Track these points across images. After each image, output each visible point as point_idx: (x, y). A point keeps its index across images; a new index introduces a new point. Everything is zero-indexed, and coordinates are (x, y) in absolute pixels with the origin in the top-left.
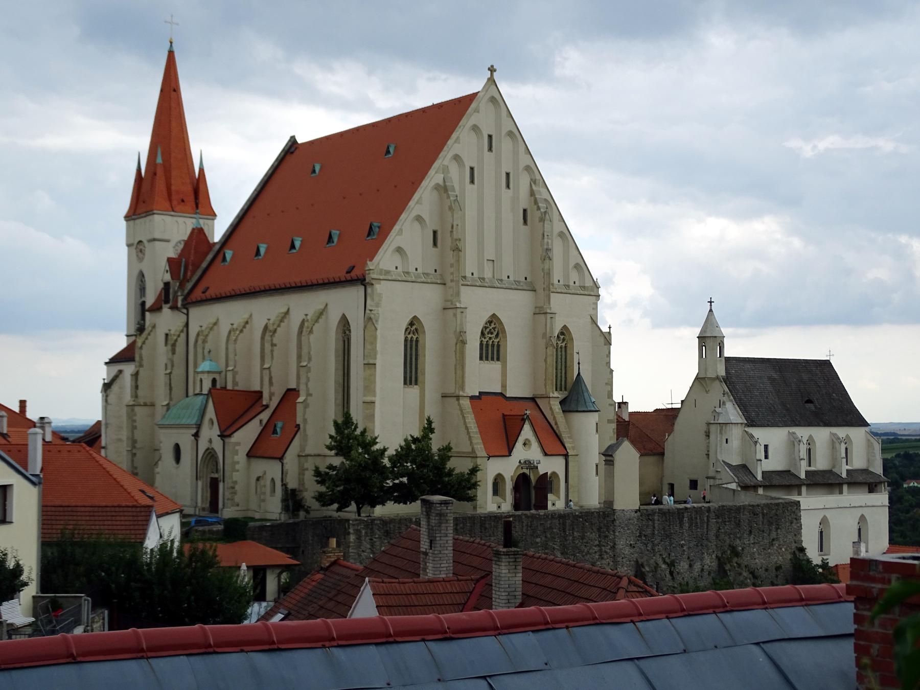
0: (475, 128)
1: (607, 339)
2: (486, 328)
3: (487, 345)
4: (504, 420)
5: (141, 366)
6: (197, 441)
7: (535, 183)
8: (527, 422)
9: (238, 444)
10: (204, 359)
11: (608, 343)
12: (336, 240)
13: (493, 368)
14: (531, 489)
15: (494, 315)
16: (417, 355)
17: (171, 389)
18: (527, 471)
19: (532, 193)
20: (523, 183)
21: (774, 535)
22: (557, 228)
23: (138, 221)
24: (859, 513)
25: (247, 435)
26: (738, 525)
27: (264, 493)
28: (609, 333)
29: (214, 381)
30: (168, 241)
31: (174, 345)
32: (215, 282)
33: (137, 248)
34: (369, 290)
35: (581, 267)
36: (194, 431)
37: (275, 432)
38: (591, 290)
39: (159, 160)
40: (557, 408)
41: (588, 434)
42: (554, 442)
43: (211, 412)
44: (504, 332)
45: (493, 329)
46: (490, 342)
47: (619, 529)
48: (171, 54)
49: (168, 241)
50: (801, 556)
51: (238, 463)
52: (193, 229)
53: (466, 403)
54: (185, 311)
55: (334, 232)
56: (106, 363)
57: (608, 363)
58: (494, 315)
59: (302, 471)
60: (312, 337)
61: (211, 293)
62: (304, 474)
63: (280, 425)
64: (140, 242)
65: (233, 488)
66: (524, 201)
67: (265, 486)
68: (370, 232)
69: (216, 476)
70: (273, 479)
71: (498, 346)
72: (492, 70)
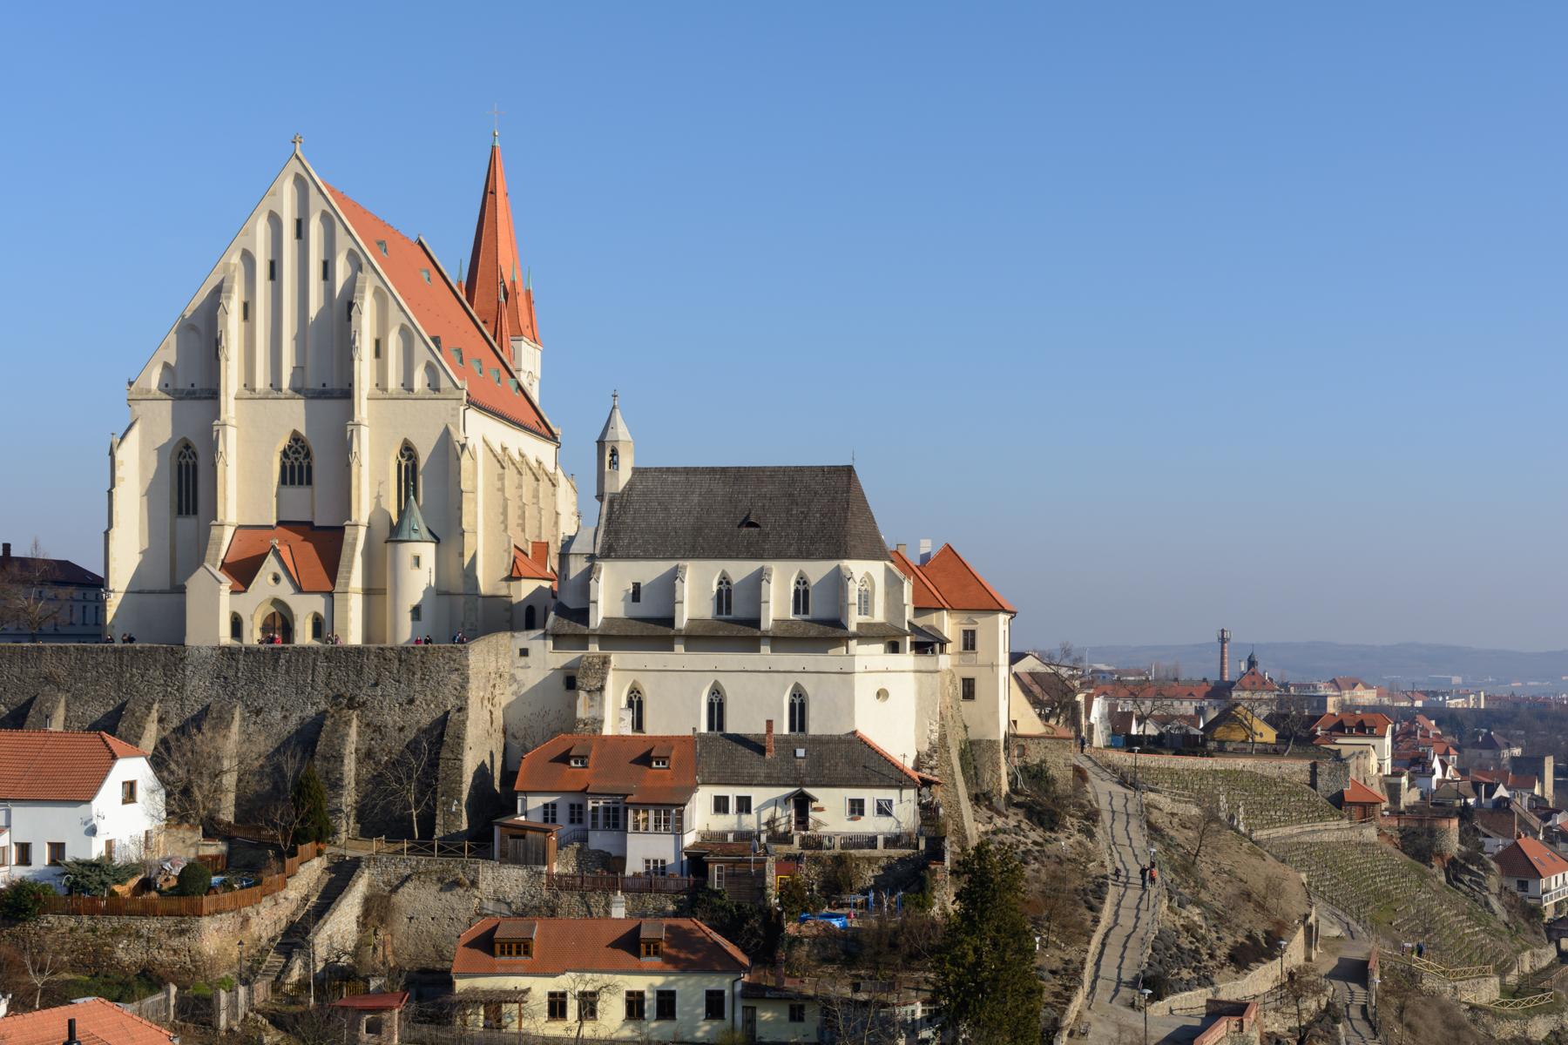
3: (292, 467)
13: (297, 493)
24: (791, 681)
26: (359, 673)
50: (454, 716)
71: (309, 468)
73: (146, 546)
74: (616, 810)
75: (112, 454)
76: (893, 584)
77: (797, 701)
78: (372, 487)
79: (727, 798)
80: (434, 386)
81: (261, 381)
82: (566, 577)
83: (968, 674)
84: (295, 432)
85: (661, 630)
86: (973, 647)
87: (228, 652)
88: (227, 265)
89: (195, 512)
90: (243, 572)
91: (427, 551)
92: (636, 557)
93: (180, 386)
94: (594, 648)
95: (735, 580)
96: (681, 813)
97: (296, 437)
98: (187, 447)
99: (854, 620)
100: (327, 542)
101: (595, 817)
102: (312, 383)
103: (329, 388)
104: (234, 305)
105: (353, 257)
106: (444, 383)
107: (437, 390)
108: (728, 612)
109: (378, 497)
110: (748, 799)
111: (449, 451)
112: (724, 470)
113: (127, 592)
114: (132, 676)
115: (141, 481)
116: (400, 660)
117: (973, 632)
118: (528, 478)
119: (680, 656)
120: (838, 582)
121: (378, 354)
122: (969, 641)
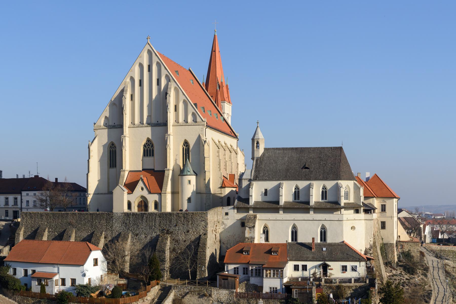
3: (147, 150)
13: (149, 159)
21: (190, 226)
24: (321, 223)
26: (170, 222)
46: (149, 149)
47: (115, 220)
50: (203, 237)
71: (153, 150)
73: (100, 179)
74: (259, 270)
75: (89, 148)
76: (357, 189)
77: (323, 231)
78: (174, 157)
79: (298, 265)
80: (195, 121)
81: (137, 121)
82: (241, 187)
83: (383, 220)
84: (148, 138)
85: (275, 206)
86: (385, 211)
87: (127, 215)
88: (126, 82)
89: (115, 166)
90: (131, 187)
91: (193, 179)
92: (266, 180)
93: (110, 124)
94: (251, 212)
95: (301, 187)
96: (282, 271)
97: (148, 140)
98: (113, 144)
99: (343, 202)
100: (158, 175)
101: (252, 272)
102: (154, 121)
103: (159, 123)
104: (128, 96)
105: (167, 76)
106: (198, 119)
107: (196, 122)
108: (298, 199)
109: (176, 160)
110: (306, 266)
111: (200, 143)
112: (296, 149)
113: (94, 194)
114: (96, 223)
115: (98, 156)
116: (184, 217)
117: (385, 205)
118: (227, 152)
119: (281, 215)
120: (337, 188)
121: (132, 99)
122: (383, 208)
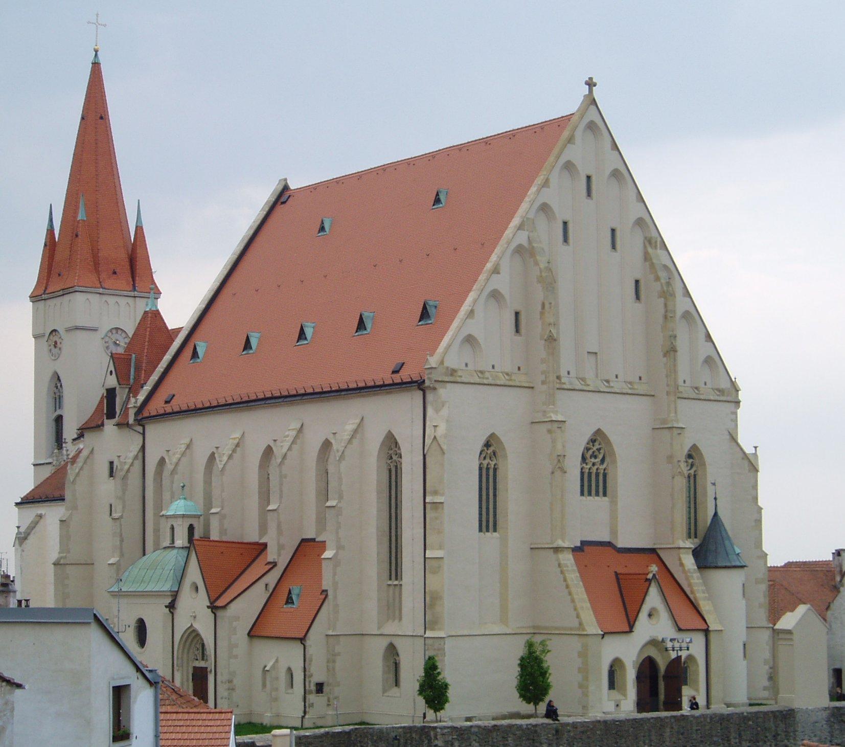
0: (569, 166)
1: (750, 465)
2: (588, 449)
3: (590, 474)
4: (624, 578)
5: (75, 508)
6: (172, 613)
7: (650, 243)
8: (653, 584)
9: (237, 618)
10: (173, 498)
11: (755, 469)
12: (369, 325)
14: (660, 681)
15: (599, 432)
16: (495, 489)
17: (122, 541)
18: (653, 653)
19: (647, 257)
20: (631, 243)
22: (681, 306)
23: (49, 302)
25: (246, 607)
27: (277, 689)
28: (755, 454)
29: (191, 529)
30: (94, 330)
31: (125, 478)
32: (185, 387)
33: (50, 340)
34: (430, 397)
35: (714, 361)
36: (168, 601)
37: (289, 600)
38: (729, 395)
39: (81, 216)
40: (689, 561)
41: (728, 600)
42: (688, 610)
43: (194, 574)
44: (613, 454)
45: (597, 448)
46: (594, 470)
48: (96, 66)
49: (94, 330)
51: (236, 646)
52: (146, 312)
53: (568, 559)
54: (140, 429)
55: (365, 314)
56: (17, 504)
57: (756, 498)
58: (599, 432)
59: (332, 658)
60: (343, 465)
61: (175, 405)
62: (334, 661)
63: (295, 591)
64: (55, 331)
65: (230, 681)
66: (637, 269)
67: (277, 678)
68: (425, 314)
69: (202, 664)
70: (289, 669)
71: (605, 475)
72: (591, 84)
